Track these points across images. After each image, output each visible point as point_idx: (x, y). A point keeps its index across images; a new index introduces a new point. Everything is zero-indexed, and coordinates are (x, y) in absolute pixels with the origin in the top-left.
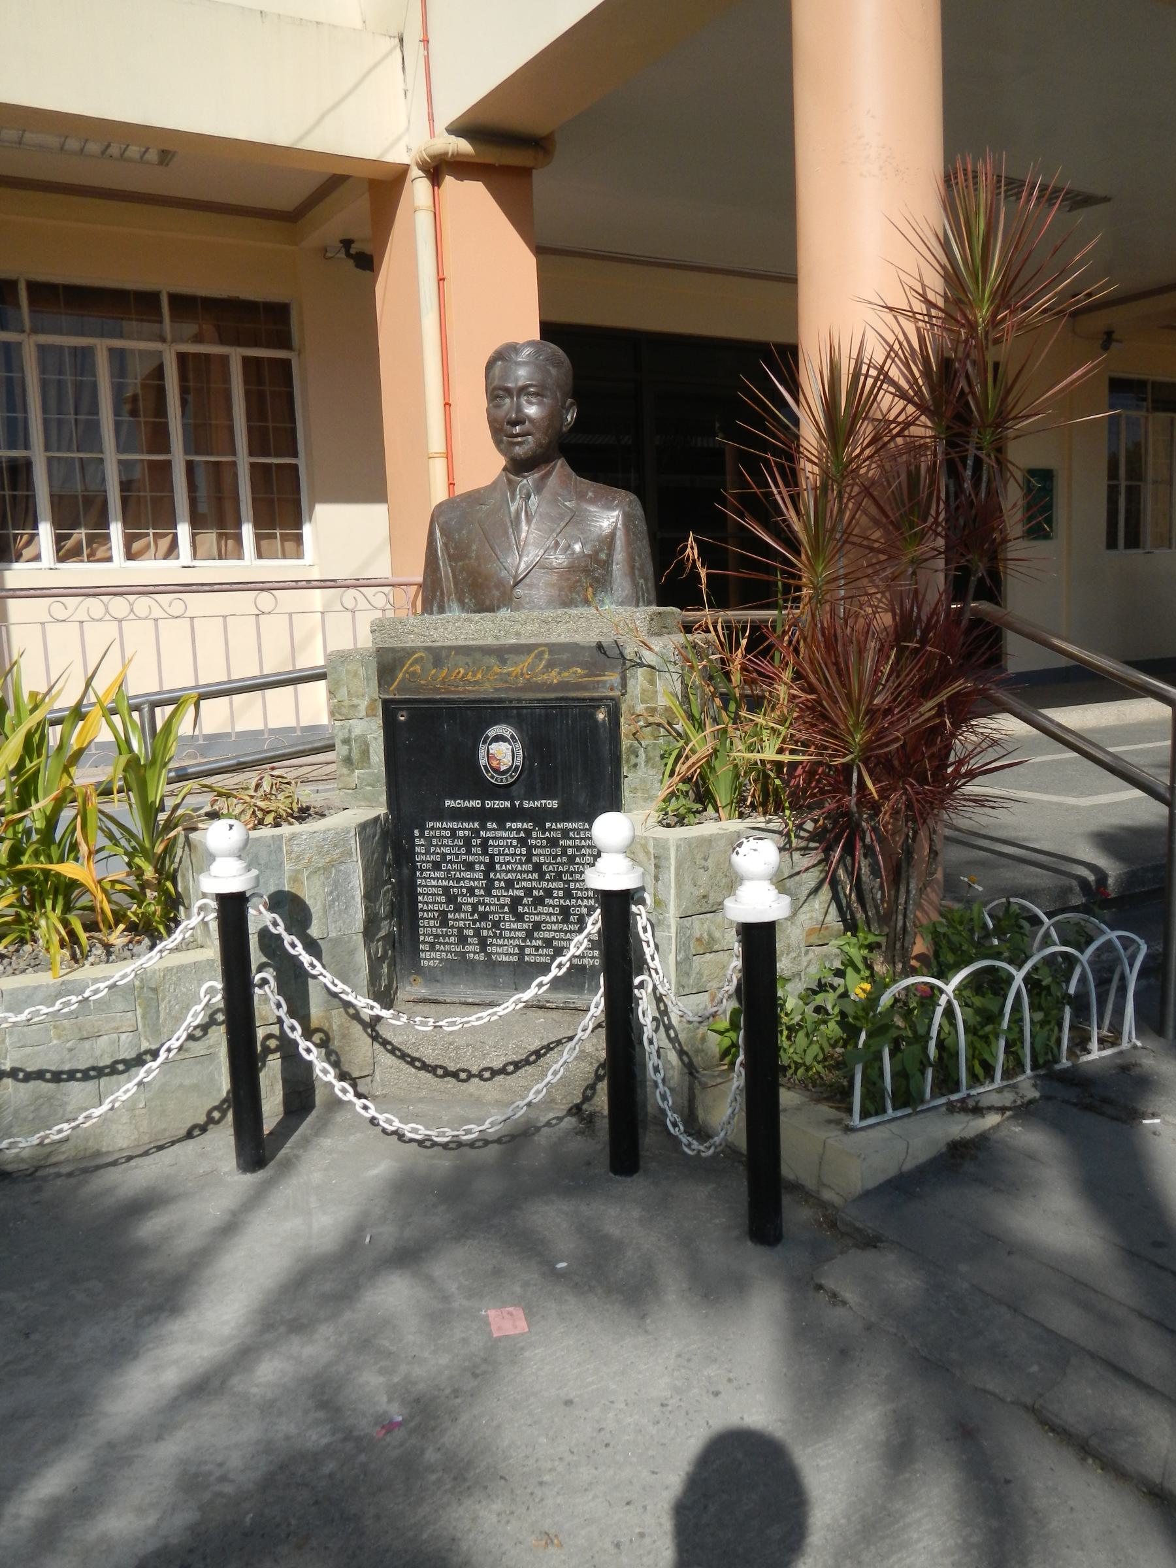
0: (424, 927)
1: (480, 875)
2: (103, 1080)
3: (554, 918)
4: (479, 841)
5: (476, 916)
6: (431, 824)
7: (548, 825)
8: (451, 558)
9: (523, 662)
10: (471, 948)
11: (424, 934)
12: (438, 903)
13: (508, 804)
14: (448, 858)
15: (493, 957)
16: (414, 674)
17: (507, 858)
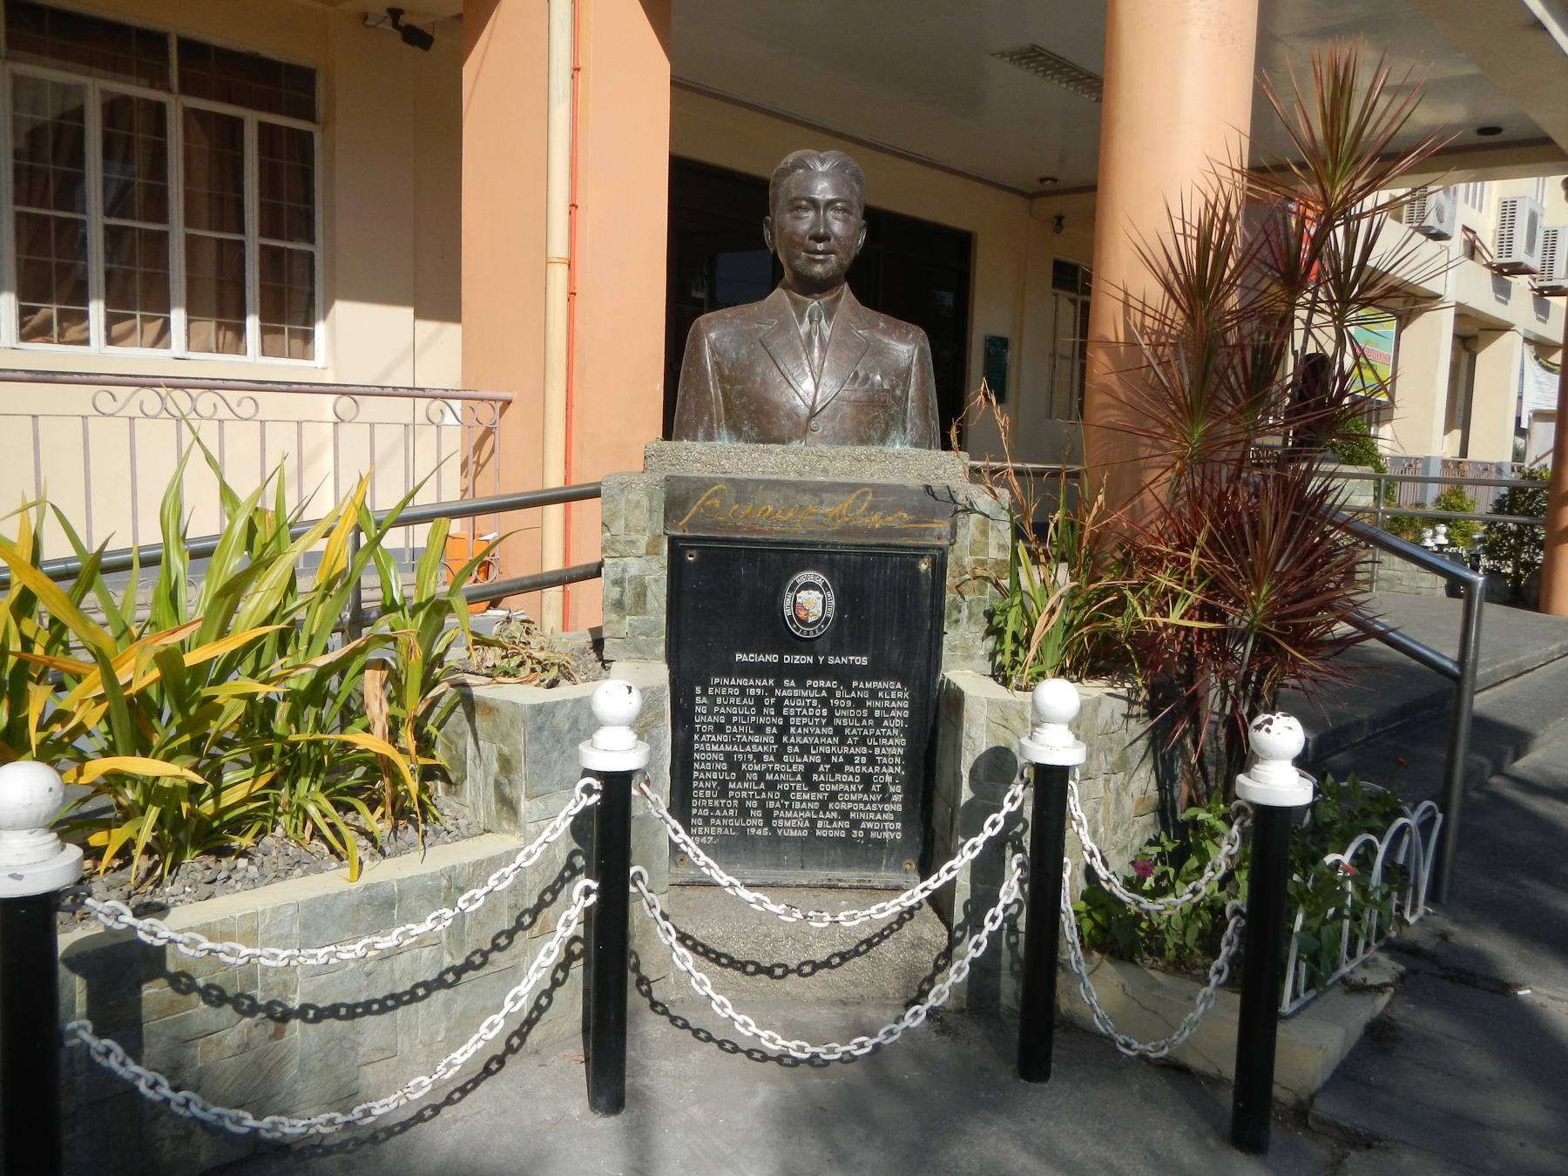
0: (698, 798)
1: (771, 740)
2: (400, 1011)
3: (853, 788)
4: (773, 700)
5: (762, 786)
6: (717, 680)
7: (855, 684)
8: (722, 379)
9: (843, 502)
10: (754, 822)
11: (697, 807)
12: (718, 770)
13: (810, 660)
14: (735, 719)
15: (780, 832)
16: (711, 509)
17: (805, 720)
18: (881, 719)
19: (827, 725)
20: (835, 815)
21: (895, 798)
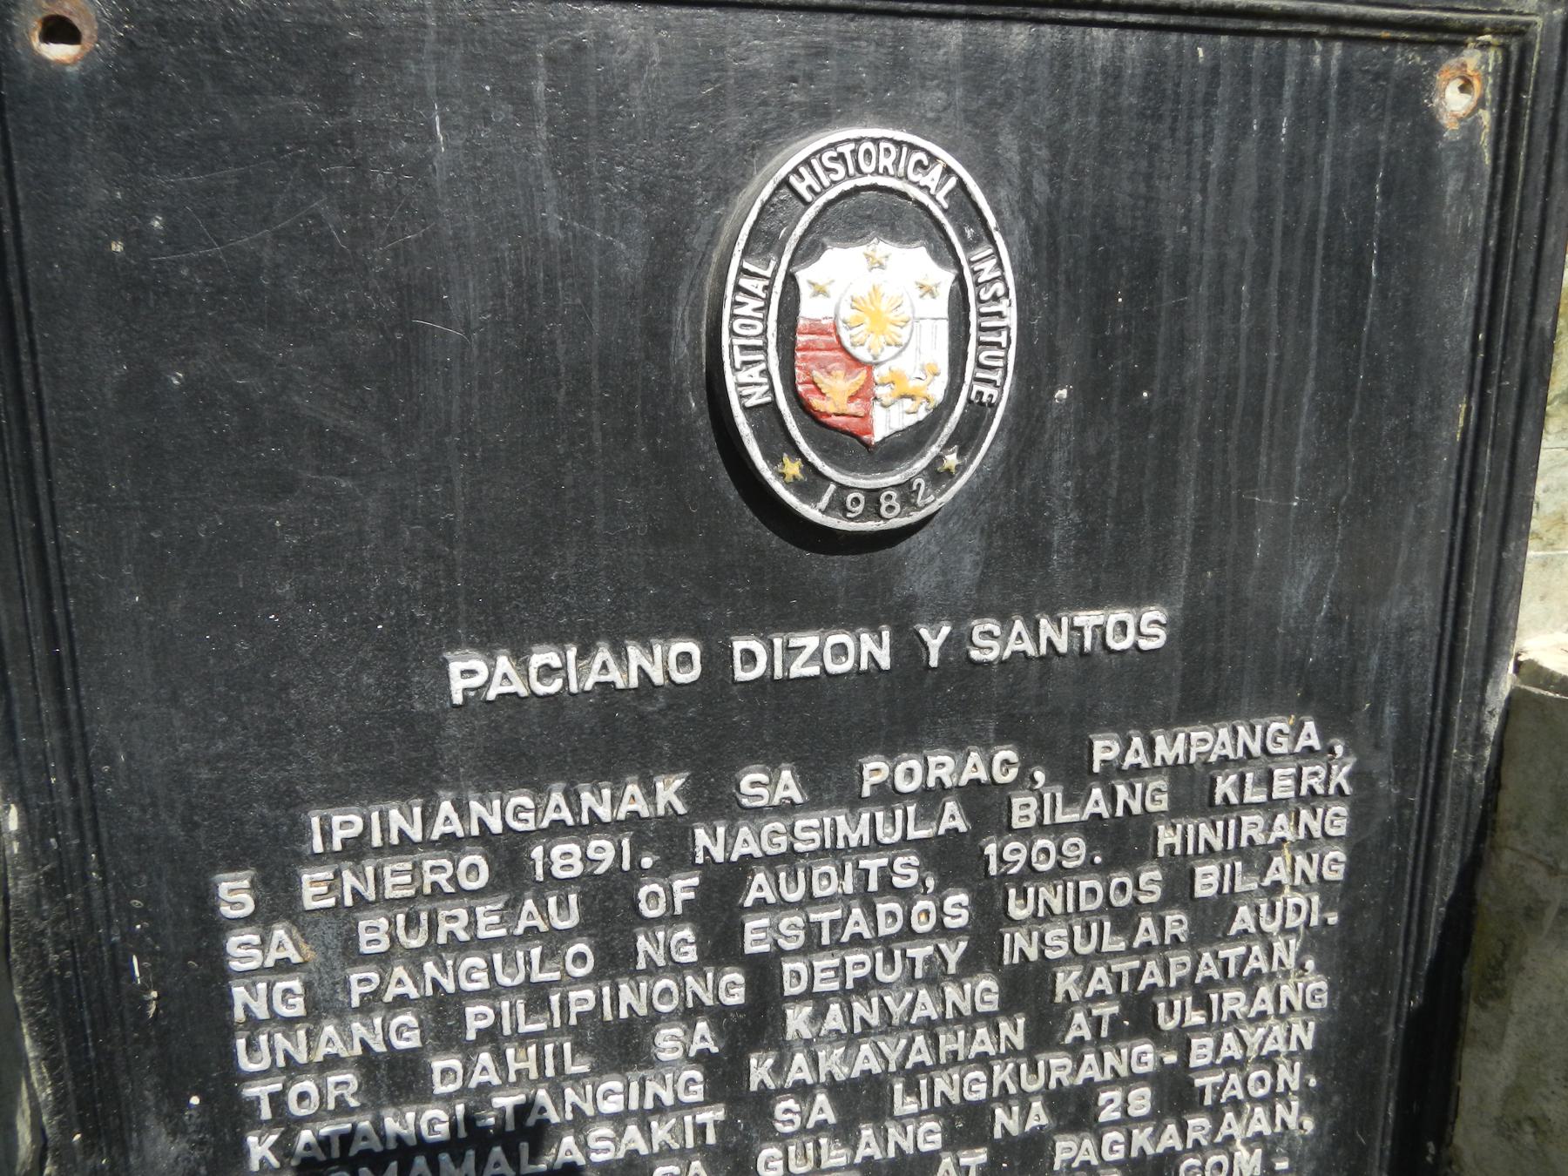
4: (685, 887)
6: (346, 824)
7: (1104, 749)
17: (857, 963)
18: (1224, 905)
19: (970, 965)
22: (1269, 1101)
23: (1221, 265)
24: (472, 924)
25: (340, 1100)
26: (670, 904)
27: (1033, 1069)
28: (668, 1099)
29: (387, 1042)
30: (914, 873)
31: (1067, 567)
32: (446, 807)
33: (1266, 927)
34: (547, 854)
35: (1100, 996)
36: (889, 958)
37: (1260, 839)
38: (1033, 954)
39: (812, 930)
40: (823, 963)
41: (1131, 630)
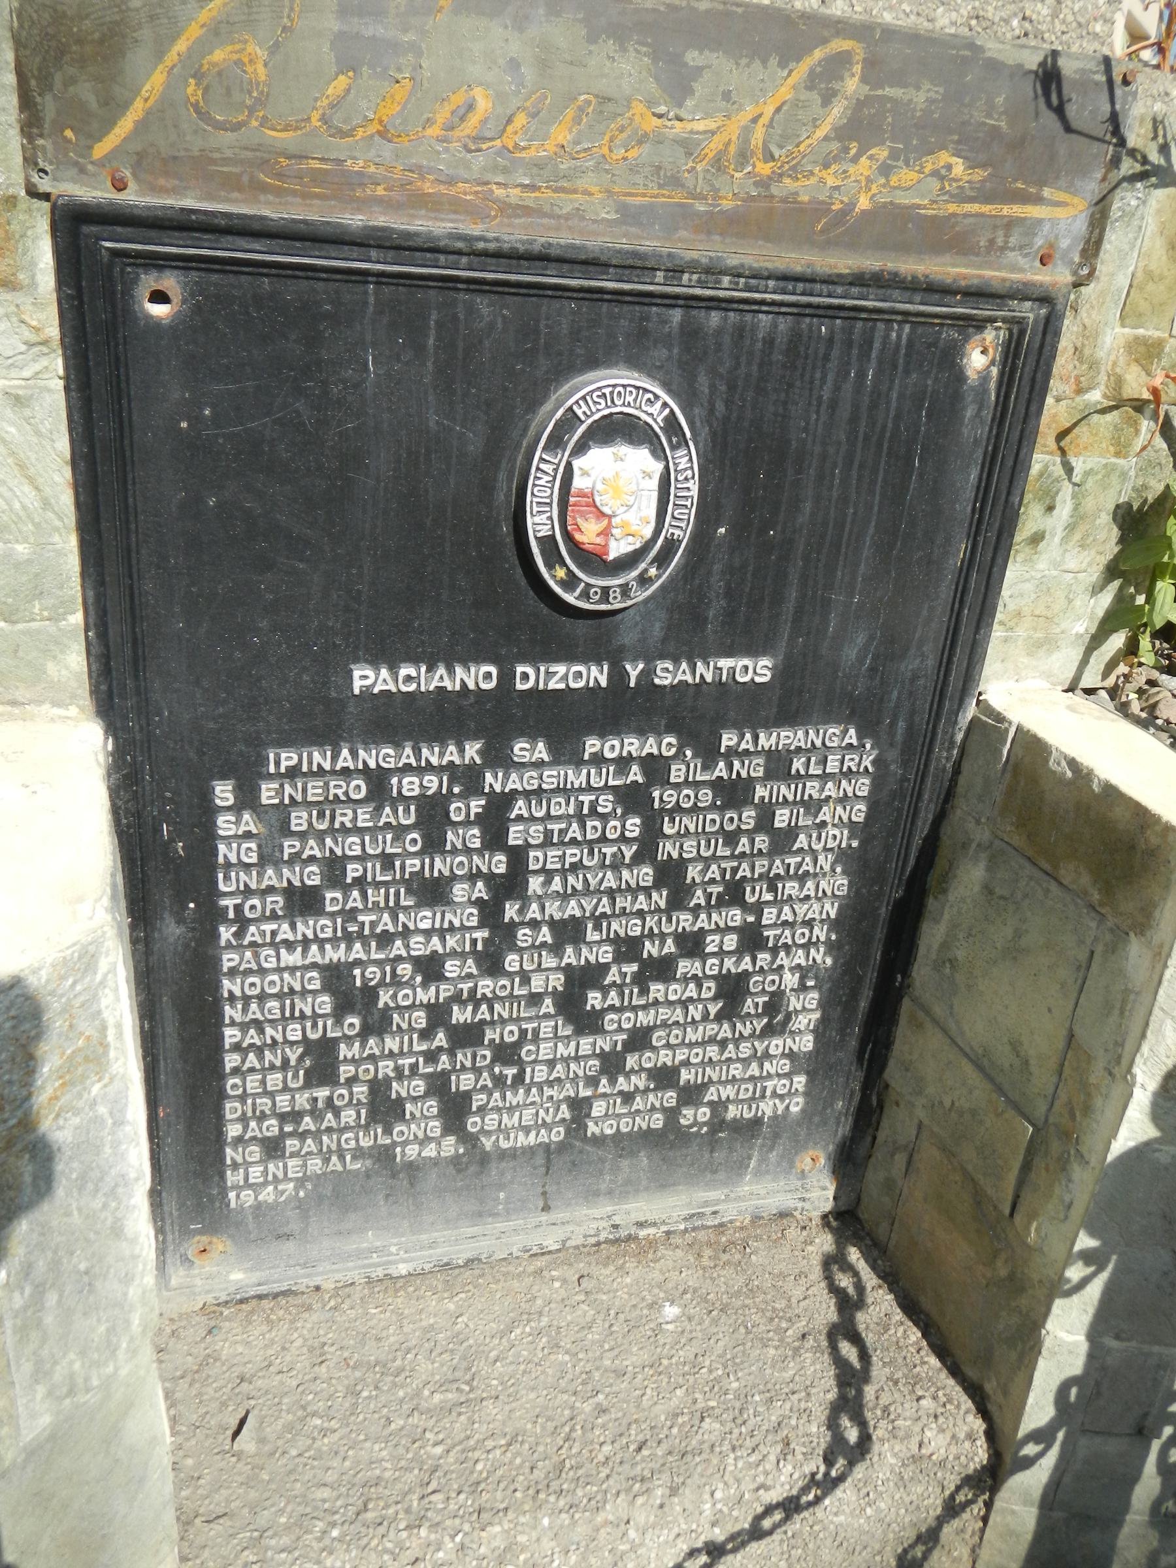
4: (477, 805)
5: (441, 1039)
6: (288, 758)
7: (728, 739)
13: (599, 675)
15: (488, 1143)
17: (573, 854)
18: (791, 832)
19: (638, 859)
20: (640, 1081)
21: (802, 1022)
22: (806, 947)
23: (824, 457)
24: (355, 818)
25: (273, 911)
26: (468, 815)
27: (670, 920)
28: (457, 923)
29: (302, 881)
30: (610, 805)
31: (716, 632)
32: (345, 752)
33: (814, 846)
34: (400, 782)
35: (713, 881)
36: (591, 853)
37: (816, 796)
38: (675, 855)
39: (548, 834)
40: (553, 853)
41: (751, 671)
